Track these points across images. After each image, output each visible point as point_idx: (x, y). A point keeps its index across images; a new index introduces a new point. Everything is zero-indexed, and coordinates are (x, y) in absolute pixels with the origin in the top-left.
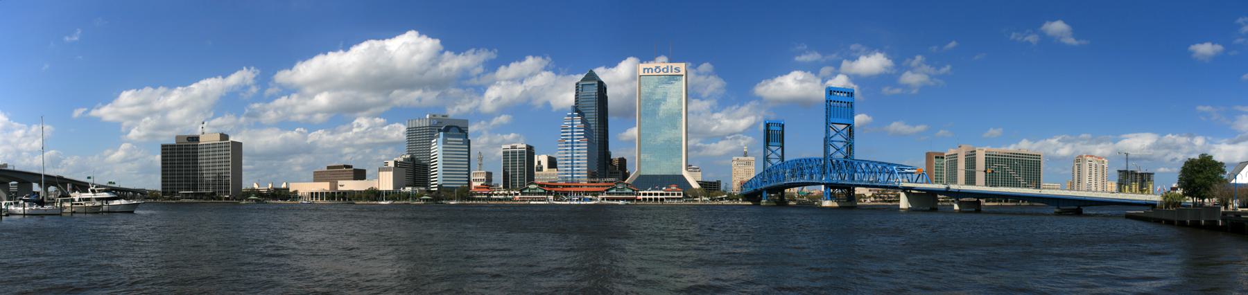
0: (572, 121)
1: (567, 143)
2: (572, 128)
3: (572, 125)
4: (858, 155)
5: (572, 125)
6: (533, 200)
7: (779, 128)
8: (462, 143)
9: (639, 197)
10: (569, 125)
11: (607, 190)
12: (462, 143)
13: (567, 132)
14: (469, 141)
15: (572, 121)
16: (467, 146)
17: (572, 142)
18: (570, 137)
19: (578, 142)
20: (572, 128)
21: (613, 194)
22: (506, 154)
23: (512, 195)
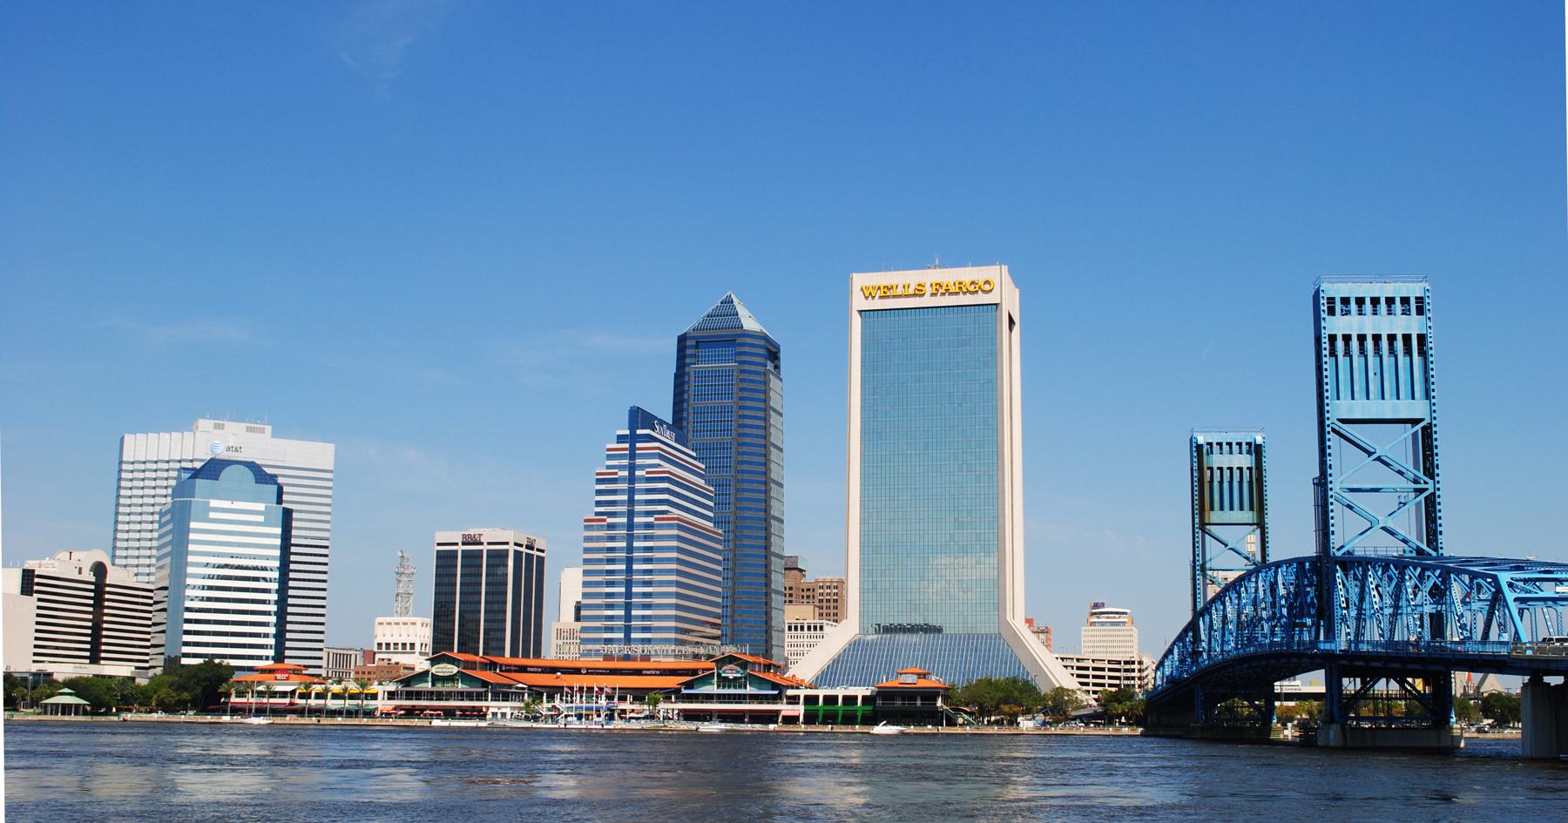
0: (633, 456)
1: (612, 526)
2: (632, 479)
3: (632, 468)
4: (1453, 544)
5: (632, 468)
6: (438, 716)
7: (1246, 461)
8: (261, 519)
9: (786, 709)
10: (621, 468)
11: (689, 685)
12: (261, 519)
13: (614, 492)
14: (288, 513)
15: (633, 456)
16: (279, 531)
17: (630, 526)
18: (637, 508)
19: (649, 526)
20: (632, 479)
21: (709, 698)
22: (445, 560)
23: (374, 696)
